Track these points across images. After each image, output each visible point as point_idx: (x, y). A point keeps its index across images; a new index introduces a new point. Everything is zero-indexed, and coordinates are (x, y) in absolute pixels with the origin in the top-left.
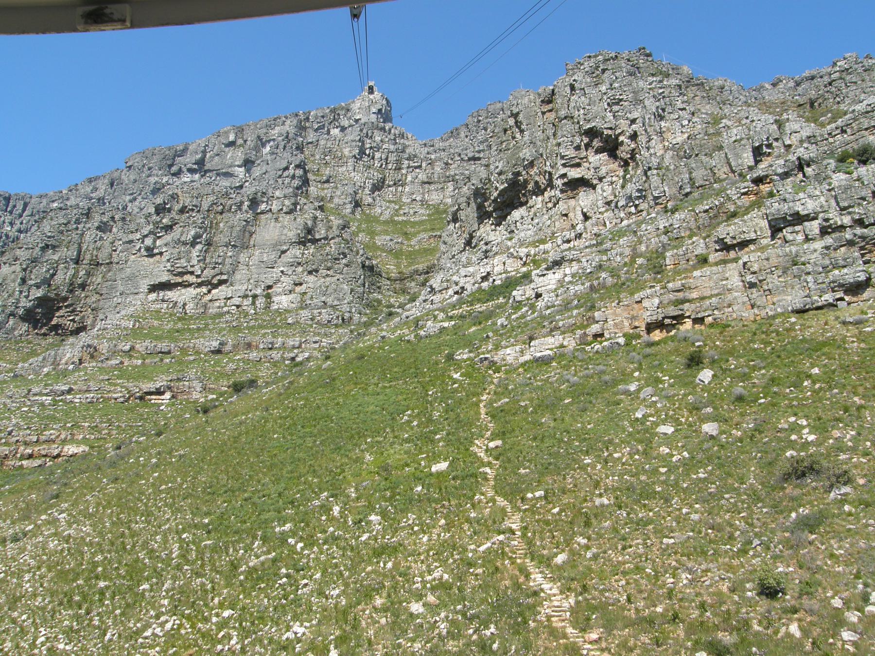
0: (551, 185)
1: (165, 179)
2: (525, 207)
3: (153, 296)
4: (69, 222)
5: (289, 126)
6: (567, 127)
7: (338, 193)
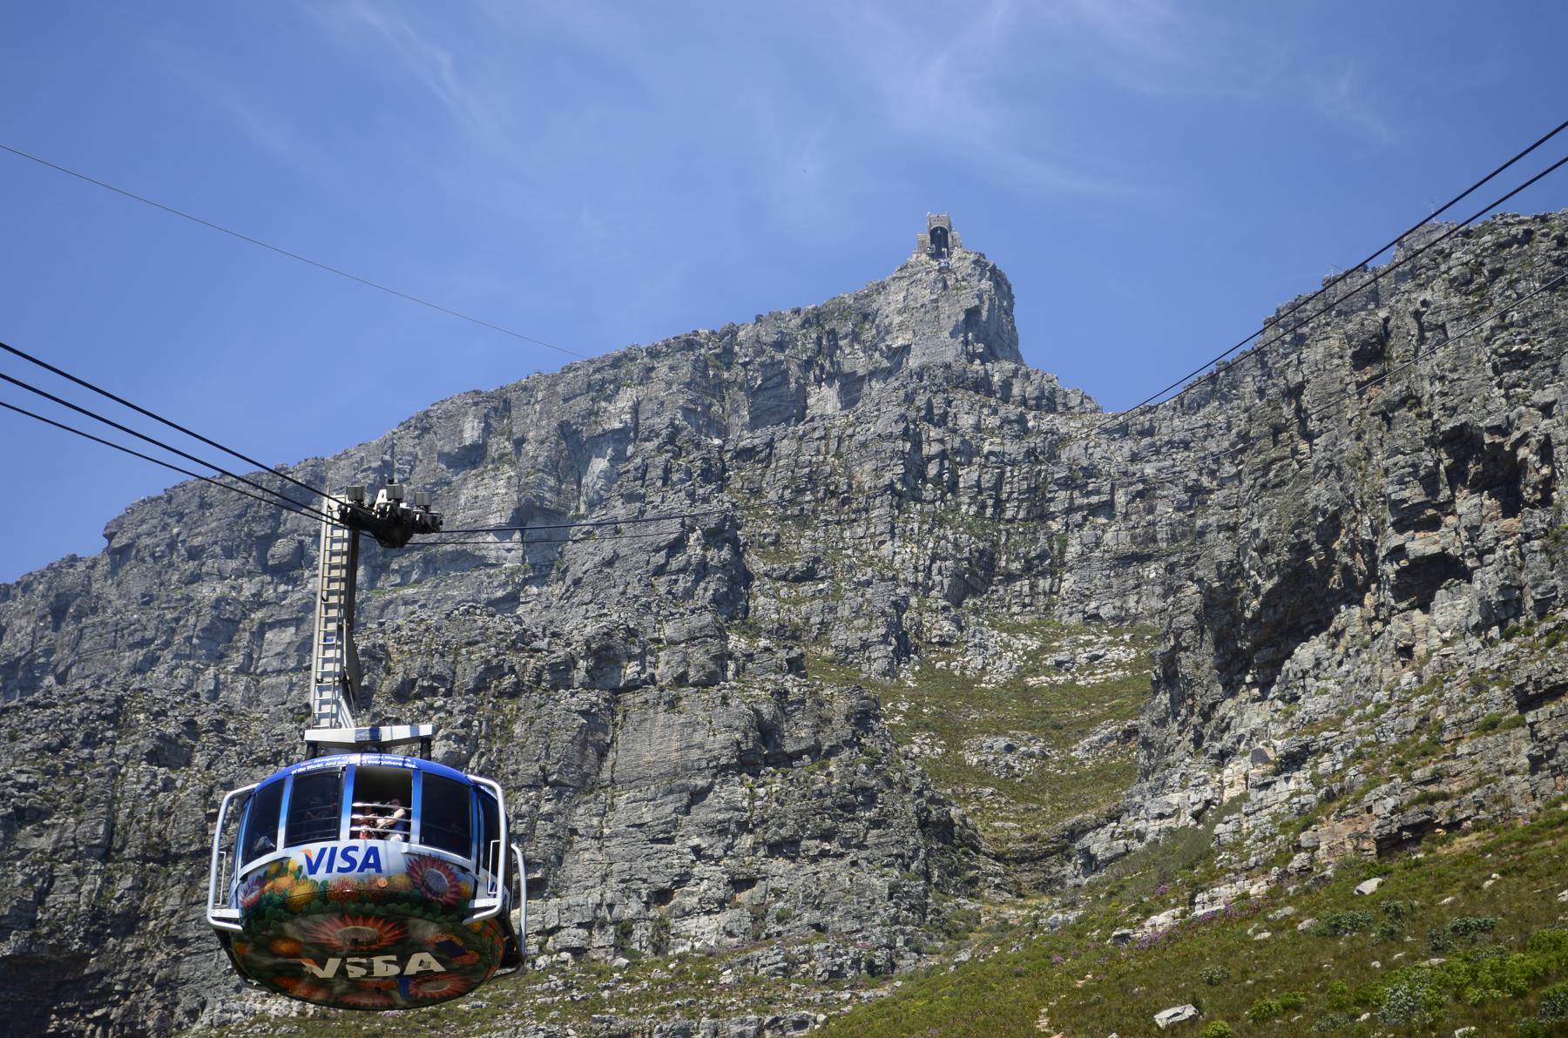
0: (1373, 576)
2: (1323, 635)
4: (64, 743)
6: (1409, 427)
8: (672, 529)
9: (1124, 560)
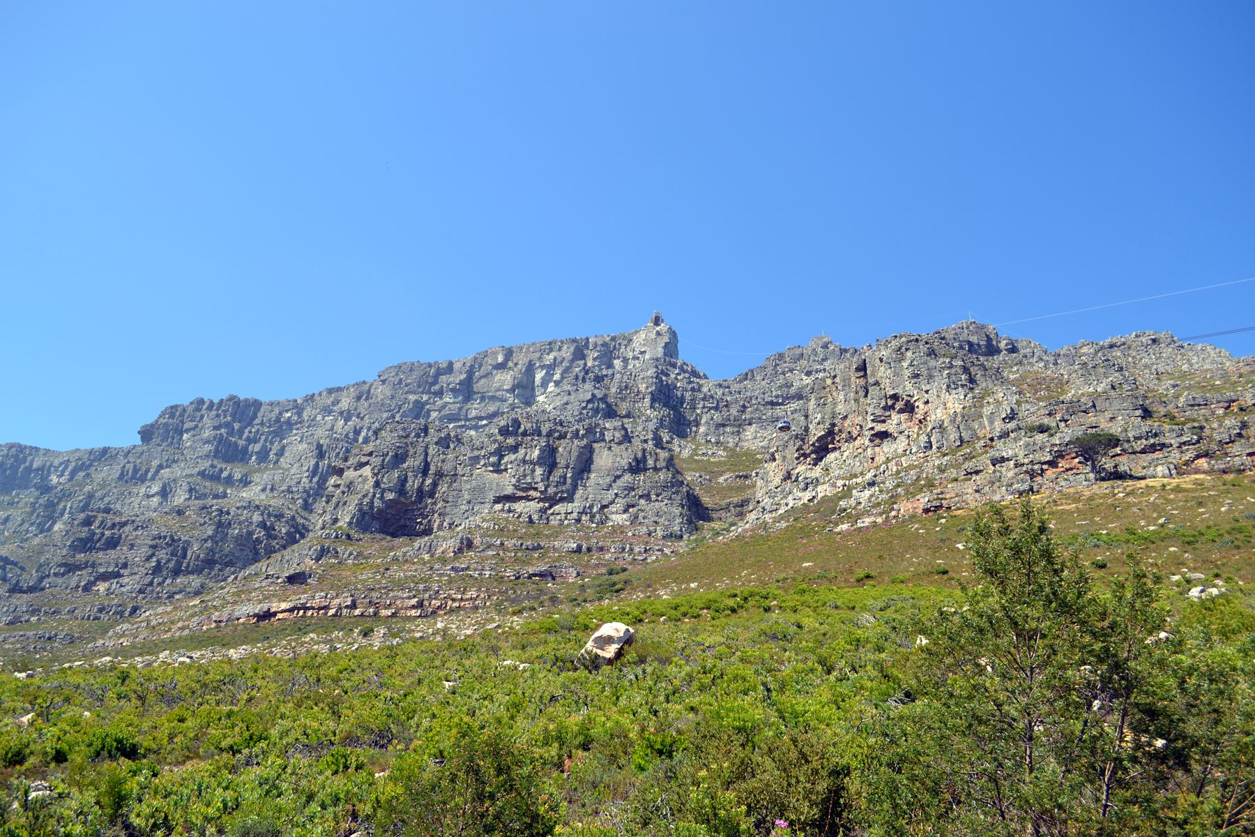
1: (425, 398)
3: (498, 507)
4: (407, 437)
5: (567, 352)
7: (640, 429)
8: (589, 396)
9: (719, 426)
